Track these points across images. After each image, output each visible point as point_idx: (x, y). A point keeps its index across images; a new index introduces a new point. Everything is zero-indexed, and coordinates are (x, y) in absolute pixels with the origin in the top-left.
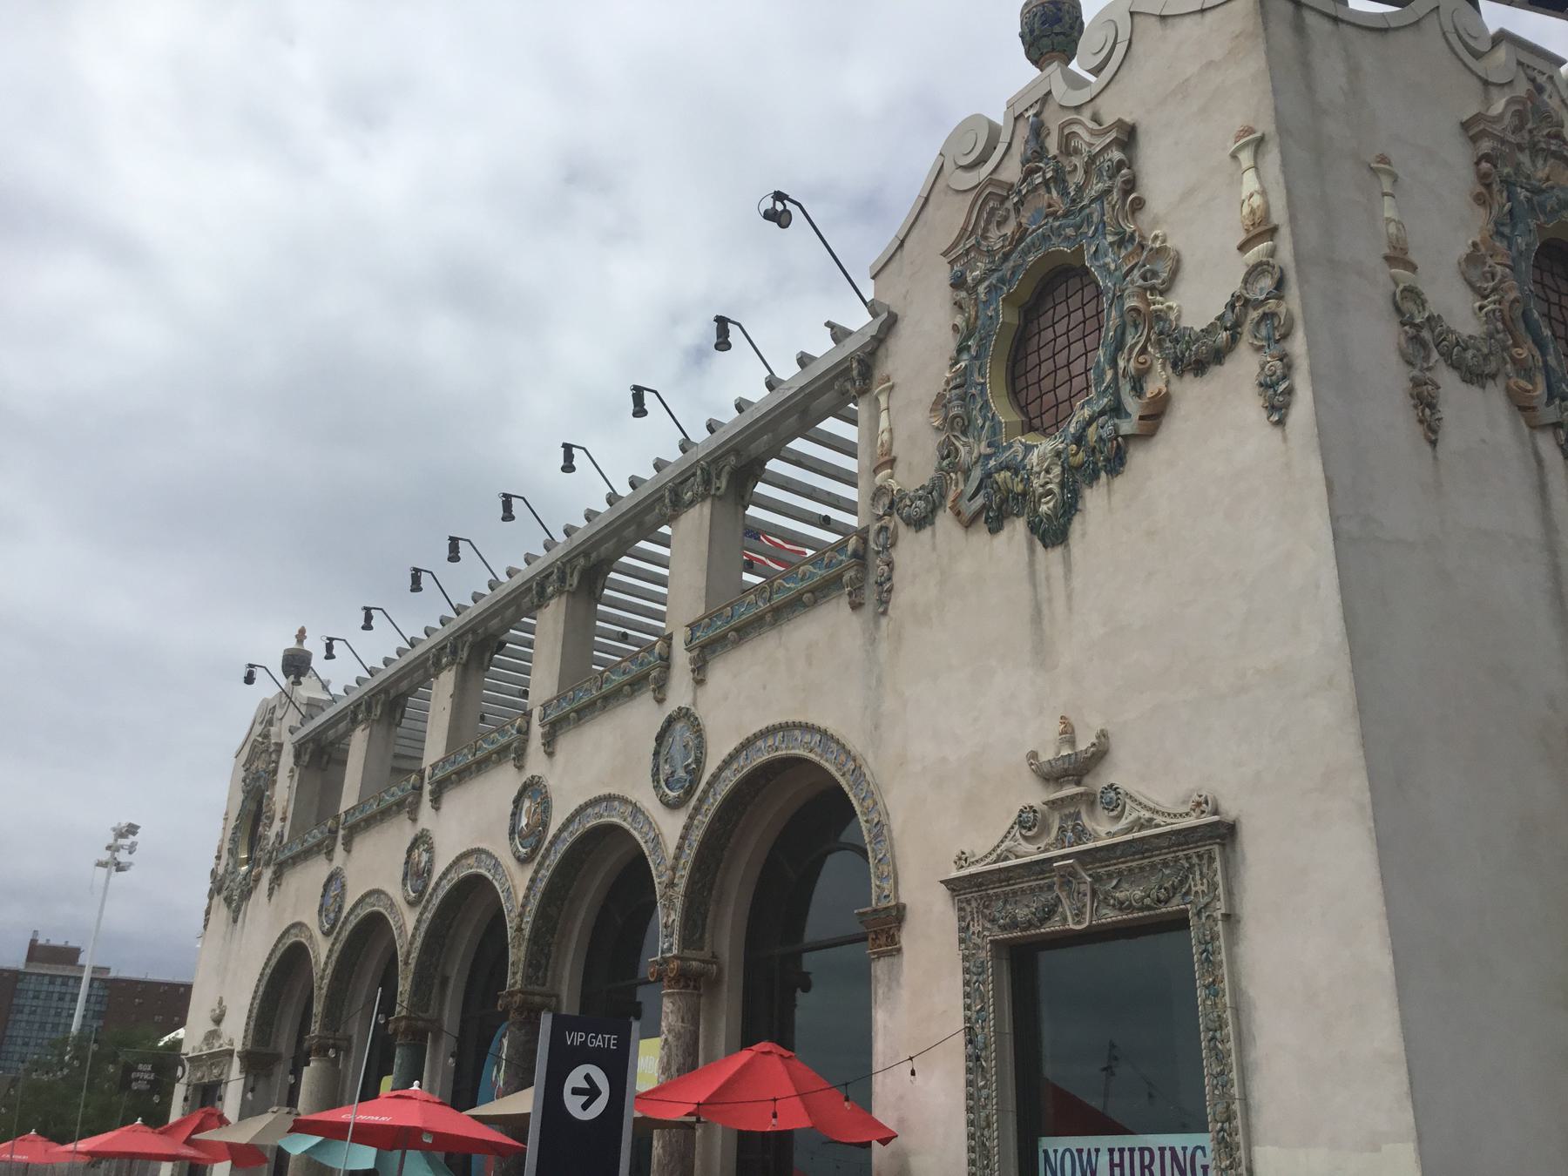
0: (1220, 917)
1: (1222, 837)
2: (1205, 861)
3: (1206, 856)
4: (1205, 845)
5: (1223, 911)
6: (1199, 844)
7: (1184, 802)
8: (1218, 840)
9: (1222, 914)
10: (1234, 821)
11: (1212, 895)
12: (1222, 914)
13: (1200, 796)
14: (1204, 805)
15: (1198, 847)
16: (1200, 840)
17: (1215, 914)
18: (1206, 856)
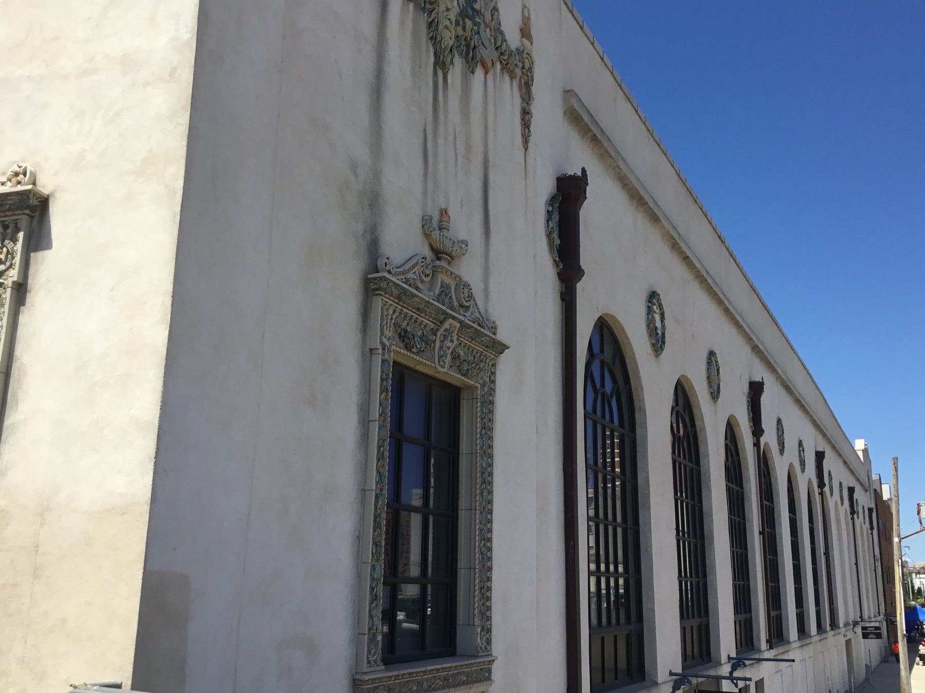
0: (10, 285)
1: (33, 209)
2: (9, 231)
3: (11, 226)
4: (15, 215)
5: (15, 279)
6: (8, 213)
7: (4, 174)
8: (27, 212)
9: (13, 282)
10: (48, 196)
11: (8, 264)
12: (13, 282)
13: (20, 167)
14: (21, 176)
15: (6, 216)
16: (9, 210)
17: (6, 282)
18: (11, 226)
